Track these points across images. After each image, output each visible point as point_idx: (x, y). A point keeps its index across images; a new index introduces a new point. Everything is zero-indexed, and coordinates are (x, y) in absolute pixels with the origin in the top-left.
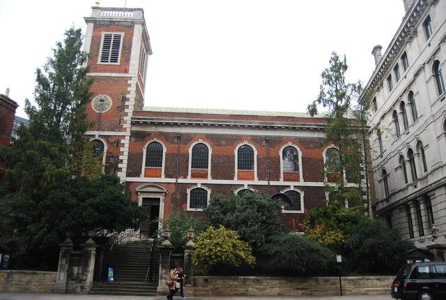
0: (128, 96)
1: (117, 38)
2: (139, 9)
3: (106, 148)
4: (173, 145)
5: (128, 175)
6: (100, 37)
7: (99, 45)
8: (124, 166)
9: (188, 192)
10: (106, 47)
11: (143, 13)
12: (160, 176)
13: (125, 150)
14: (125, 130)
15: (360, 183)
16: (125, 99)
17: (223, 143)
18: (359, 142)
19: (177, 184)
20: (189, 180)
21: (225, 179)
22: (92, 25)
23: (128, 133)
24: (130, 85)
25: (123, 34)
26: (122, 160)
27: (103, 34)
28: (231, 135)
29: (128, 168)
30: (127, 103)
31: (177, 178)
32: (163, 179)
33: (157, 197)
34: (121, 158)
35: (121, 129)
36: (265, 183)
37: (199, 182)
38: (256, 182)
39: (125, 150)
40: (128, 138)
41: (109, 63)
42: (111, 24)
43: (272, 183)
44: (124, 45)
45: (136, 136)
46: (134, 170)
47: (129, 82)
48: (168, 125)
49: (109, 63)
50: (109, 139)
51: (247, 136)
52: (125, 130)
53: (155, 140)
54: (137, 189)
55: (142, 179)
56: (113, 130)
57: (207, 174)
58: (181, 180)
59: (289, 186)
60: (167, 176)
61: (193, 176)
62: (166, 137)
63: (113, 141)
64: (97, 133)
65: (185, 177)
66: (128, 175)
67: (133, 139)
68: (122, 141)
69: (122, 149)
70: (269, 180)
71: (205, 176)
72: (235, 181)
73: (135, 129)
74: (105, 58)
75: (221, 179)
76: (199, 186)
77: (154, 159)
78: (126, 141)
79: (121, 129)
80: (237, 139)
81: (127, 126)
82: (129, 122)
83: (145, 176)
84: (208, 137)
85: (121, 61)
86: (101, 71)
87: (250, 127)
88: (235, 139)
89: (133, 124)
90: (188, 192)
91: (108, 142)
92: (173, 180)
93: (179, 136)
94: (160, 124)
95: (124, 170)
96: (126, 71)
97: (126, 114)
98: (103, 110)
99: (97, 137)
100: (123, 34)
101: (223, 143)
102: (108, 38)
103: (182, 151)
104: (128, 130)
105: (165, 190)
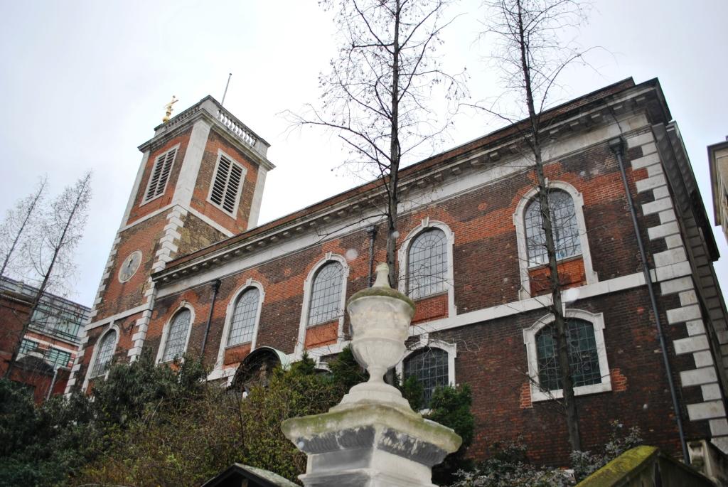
2: (203, 101)
10: (156, 177)
11: (214, 101)
13: (138, 338)
15: (650, 265)
16: (158, 247)
22: (148, 153)
30: (158, 253)
39: (138, 338)
40: (146, 314)
44: (175, 162)
53: (182, 304)
56: (132, 306)
62: (196, 294)
73: (163, 293)
78: (142, 322)
81: (149, 292)
89: (159, 285)
99: (110, 327)
100: (177, 147)
104: (149, 299)
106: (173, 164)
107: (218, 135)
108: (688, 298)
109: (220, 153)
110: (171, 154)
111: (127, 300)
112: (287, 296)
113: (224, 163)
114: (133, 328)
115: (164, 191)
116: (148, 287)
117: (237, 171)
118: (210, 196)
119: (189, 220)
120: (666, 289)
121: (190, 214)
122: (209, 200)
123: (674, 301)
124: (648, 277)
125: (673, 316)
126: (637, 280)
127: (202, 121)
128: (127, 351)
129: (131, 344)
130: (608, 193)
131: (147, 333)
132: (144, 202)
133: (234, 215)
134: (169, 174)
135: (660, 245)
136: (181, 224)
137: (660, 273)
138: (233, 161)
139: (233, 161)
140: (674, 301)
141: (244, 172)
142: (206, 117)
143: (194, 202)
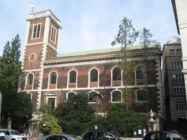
0: (43, 52)
1: (39, 25)
3: (34, 77)
4: (61, 73)
5: (43, 88)
6: (32, 27)
7: (32, 31)
8: (40, 84)
9: (67, 94)
10: (35, 31)
11: (50, 11)
12: (55, 88)
13: (41, 77)
14: (41, 68)
15: (156, 84)
16: (42, 54)
17: (83, 69)
18: (156, 61)
19: (62, 91)
20: (67, 89)
21: (84, 87)
22: (29, 22)
23: (42, 70)
24: (43, 47)
25: (41, 24)
26: (40, 82)
27: (34, 26)
28: (87, 65)
29: (43, 85)
30: (42, 56)
31: (62, 88)
32: (57, 89)
33: (54, 98)
34: (39, 81)
35: (40, 68)
36: (103, 88)
37: (72, 90)
38: (99, 88)
39: (41, 77)
40: (42, 72)
41: (36, 38)
42: (37, 20)
43: (106, 88)
45: (46, 71)
46: (45, 86)
47: (43, 46)
48: (58, 63)
49: (36, 38)
50: (35, 73)
51: (95, 64)
52: (41, 68)
54: (45, 95)
55: (48, 90)
56: (37, 69)
57: (75, 85)
58: (64, 89)
59: (115, 89)
60: (58, 88)
61: (70, 87)
63: (37, 73)
64: (30, 71)
65: (66, 88)
66: (43, 88)
67: (45, 72)
68: (40, 73)
69: (40, 77)
70: (104, 86)
71: (74, 87)
72: (89, 88)
74: (34, 36)
75: (82, 87)
76: (72, 91)
77: (53, 81)
78: (41, 73)
79: (40, 68)
80: (90, 66)
82: (42, 64)
83: (50, 88)
84: (76, 67)
85: (40, 37)
86: (32, 43)
87: (96, 60)
88: (88, 67)
90: (67, 94)
91: (34, 74)
92: (60, 90)
93: (63, 68)
94: (55, 64)
95: (41, 86)
96: (42, 41)
97: (42, 61)
98: (33, 60)
99: (30, 73)
100: (41, 24)
101: (83, 69)
102: (36, 26)
103: (64, 76)
105: (57, 95)
106: (40, 29)
107: (52, 22)
108: (160, 90)
109: (52, 26)
110: (39, 25)
111: (34, 67)
112: (84, 75)
113: (53, 28)
114: (38, 74)
115: (39, 37)
116: (41, 65)
117: (55, 30)
118: (51, 39)
119: (48, 46)
120: (158, 88)
121: (48, 45)
122: (51, 40)
123: (159, 90)
124: (155, 86)
125: (158, 92)
126: (153, 86)
127: (48, 18)
128: (38, 80)
129: (40, 79)
130: (151, 69)
131: (43, 76)
132: (32, 39)
133: (55, 43)
134: (40, 32)
135: (158, 81)
136: (47, 48)
137: (157, 85)
138: (54, 28)
139: (54, 28)
140: (159, 90)
141: (56, 31)
142: (50, 17)
143: (49, 41)
